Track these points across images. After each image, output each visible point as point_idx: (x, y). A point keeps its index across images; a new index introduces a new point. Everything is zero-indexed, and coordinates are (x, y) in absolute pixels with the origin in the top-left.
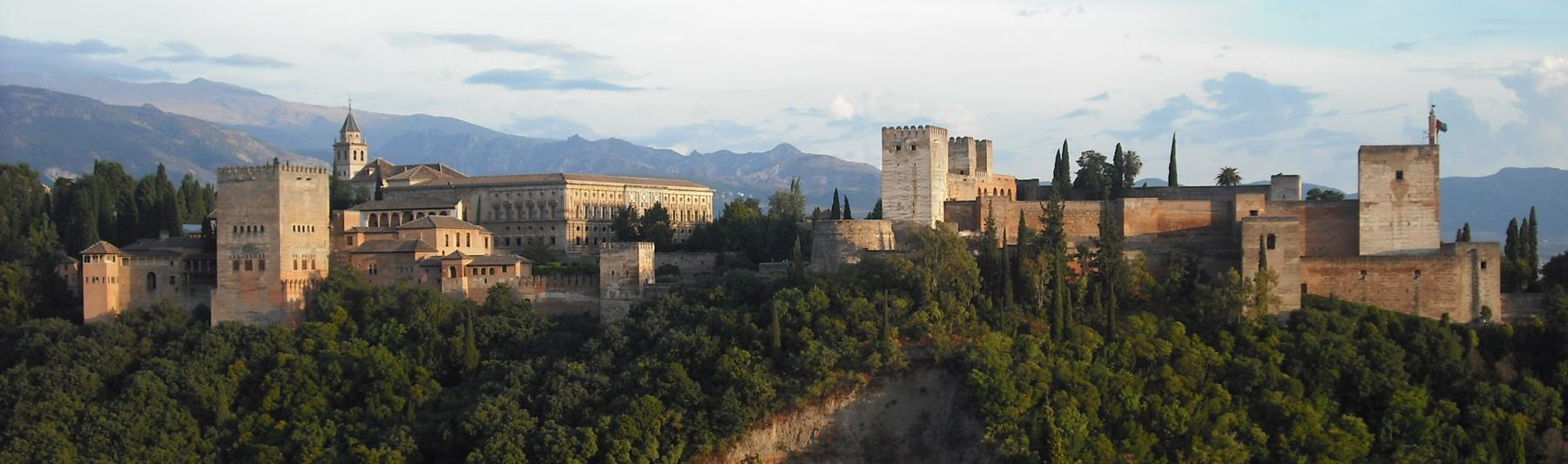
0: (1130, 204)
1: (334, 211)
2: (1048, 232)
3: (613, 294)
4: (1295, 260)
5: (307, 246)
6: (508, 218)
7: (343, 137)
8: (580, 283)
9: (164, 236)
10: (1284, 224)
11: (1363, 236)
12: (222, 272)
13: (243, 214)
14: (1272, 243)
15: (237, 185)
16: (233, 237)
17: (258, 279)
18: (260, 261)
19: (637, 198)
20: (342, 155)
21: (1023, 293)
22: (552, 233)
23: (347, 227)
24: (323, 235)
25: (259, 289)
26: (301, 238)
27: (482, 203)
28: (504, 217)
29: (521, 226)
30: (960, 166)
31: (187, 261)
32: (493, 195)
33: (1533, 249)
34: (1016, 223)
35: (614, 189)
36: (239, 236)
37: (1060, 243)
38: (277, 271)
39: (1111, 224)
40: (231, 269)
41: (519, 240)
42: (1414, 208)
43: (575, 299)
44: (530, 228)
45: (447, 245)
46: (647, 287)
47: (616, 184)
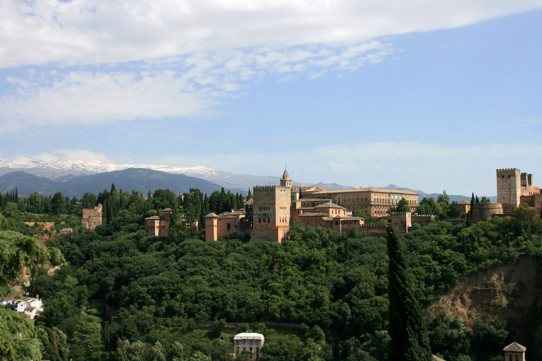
25: (268, 229)
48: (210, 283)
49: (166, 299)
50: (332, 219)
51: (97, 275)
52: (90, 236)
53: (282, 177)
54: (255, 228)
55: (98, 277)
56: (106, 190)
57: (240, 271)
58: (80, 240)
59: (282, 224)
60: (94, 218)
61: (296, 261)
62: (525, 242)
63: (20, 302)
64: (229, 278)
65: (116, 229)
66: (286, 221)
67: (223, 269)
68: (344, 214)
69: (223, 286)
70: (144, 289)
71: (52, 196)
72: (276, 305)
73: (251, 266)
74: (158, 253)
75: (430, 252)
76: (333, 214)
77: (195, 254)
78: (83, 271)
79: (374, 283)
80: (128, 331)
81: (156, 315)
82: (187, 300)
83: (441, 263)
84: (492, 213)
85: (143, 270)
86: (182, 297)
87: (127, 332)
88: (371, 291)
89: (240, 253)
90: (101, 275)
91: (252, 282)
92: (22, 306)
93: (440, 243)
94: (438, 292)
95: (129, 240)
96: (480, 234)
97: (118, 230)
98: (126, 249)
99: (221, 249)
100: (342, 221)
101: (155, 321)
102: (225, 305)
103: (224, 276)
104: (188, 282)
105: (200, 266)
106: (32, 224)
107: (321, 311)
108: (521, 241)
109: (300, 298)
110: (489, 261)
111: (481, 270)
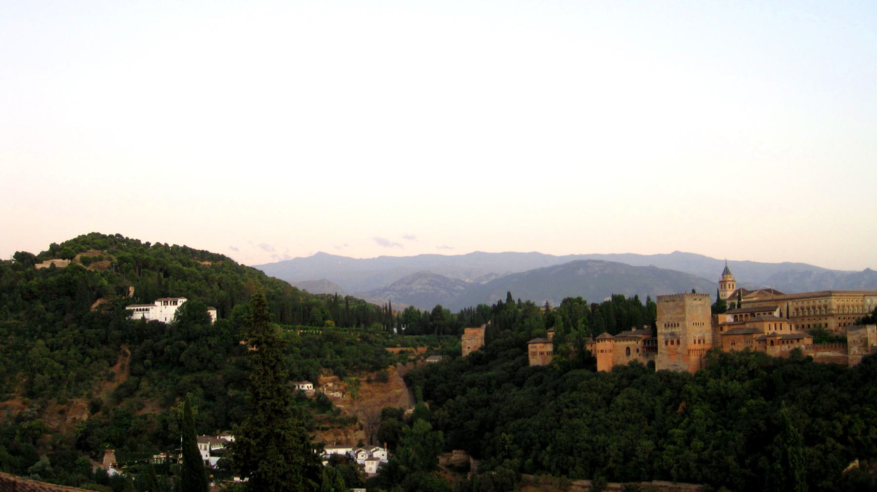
1: (714, 315)
3: (854, 352)
5: (701, 332)
6: (803, 314)
7: (723, 278)
8: (837, 347)
9: (634, 330)
12: (661, 346)
13: (669, 317)
15: (666, 303)
16: (665, 329)
17: (677, 349)
18: (675, 340)
19: (872, 301)
20: (723, 286)
22: (826, 321)
23: (720, 322)
24: (708, 326)
25: (678, 354)
26: (697, 328)
27: (790, 308)
29: (810, 318)
31: (644, 341)
32: (795, 303)
35: (858, 297)
36: (668, 329)
38: (686, 345)
40: (664, 344)
41: (809, 326)
43: (835, 355)
44: (815, 319)
45: (770, 329)
46: (873, 348)
47: (857, 295)
53: (721, 277)
54: (661, 353)
56: (501, 301)
63: (361, 451)
64: (616, 422)
66: (704, 342)
70: (508, 437)
72: (673, 459)
74: (535, 388)
92: (362, 456)
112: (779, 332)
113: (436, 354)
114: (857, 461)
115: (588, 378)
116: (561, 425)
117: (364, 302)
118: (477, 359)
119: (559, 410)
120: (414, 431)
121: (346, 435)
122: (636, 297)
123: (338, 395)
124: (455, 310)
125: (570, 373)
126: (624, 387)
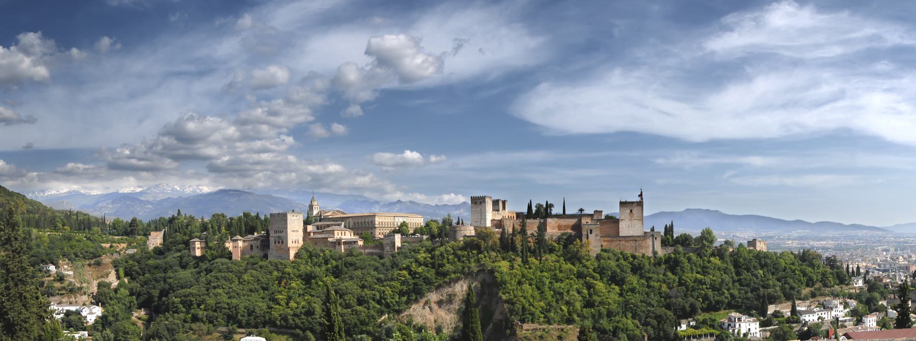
0: (549, 220)
2: (521, 229)
3: (387, 250)
4: (598, 237)
7: (311, 202)
9: (256, 234)
10: (594, 226)
11: (620, 230)
14: (591, 232)
19: (399, 220)
21: (514, 249)
22: (372, 231)
23: (308, 230)
24: (301, 234)
26: (294, 234)
28: (357, 226)
30: (497, 209)
31: (262, 241)
33: (673, 233)
34: (512, 227)
37: (525, 233)
39: (542, 228)
42: (636, 221)
48: (229, 296)
49: (194, 309)
50: (335, 241)
51: (147, 288)
52: (148, 255)
55: (148, 290)
57: (253, 285)
58: (140, 259)
59: (294, 245)
60: (152, 240)
61: (300, 276)
62: (484, 259)
65: (168, 249)
67: (240, 284)
68: (348, 236)
69: (238, 298)
70: (177, 300)
71: (130, 221)
73: (263, 281)
75: (408, 268)
76: (337, 235)
77: (220, 271)
78: (135, 285)
79: (357, 295)
80: (160, 333)
81: (185, 321)
82: (209, 309)
83: (413, 278)
84: (464, 235)
85: (179, 285)
86: (205, 307)
87: (159, 335)
88: (353, 302)
89: (256, 270)
90: (150, 288)
91: (262, 294)
93: (417, 261)
94: (408, 303)
95: (173, 259)
96: (450, 253)
97: (169, 250)
98: (171, 267)
99: (241, 266)
100: (344, 242)
101: (184, 326)
102: (237, 314)
103: (240, 290)
104: (211, 294)
105: (223, 281)
106: (108, 245)
107: (313, 319)
108: (482, 258)
109: (297, 308)
110: (453, 276)
111: (445, 282)
112: (343, 237)
113: (133, 248)
114: (387, 315)
115: (226, 264)
116: (210, 293)
117: (88, 215)
118: (159, 252)
119: (209, 283)
120: (118, 296)
121: (76, 298)
122: (258, 213)
123: (71, 273)
124: (145, 221)
125: (216, 261)
126: (248, 269)
